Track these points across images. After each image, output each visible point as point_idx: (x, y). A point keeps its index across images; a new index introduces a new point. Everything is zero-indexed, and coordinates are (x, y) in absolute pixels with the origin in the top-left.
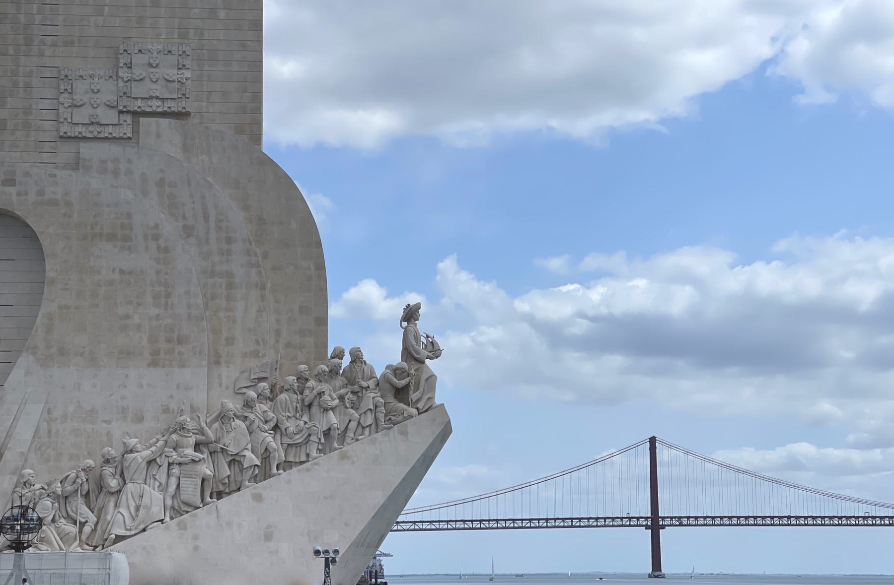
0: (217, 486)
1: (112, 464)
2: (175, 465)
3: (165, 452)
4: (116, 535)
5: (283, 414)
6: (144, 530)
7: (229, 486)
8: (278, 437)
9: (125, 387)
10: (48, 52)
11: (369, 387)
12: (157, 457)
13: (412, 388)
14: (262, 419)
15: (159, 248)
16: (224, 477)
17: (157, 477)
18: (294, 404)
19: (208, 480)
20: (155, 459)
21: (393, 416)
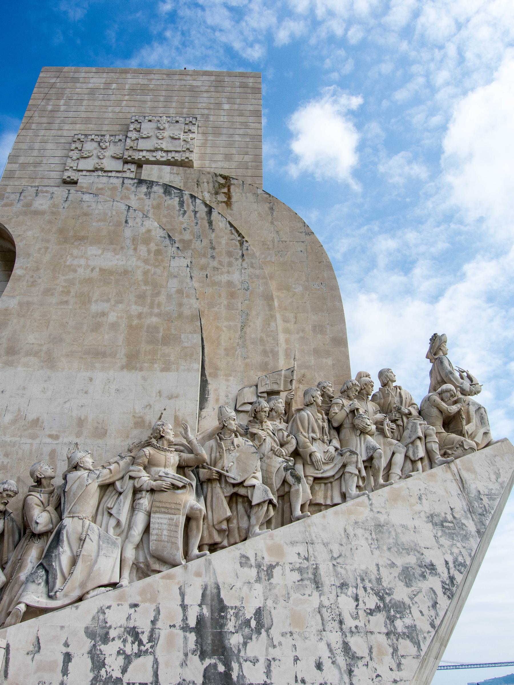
0: (210, 535)
1: (45, 488)
2: (144, 493)
3: (130, 471)
4: (27, 606)
5: (306, 434)
6: (80, 599)
7: (228, 536)
8: (299, 467)
9: (86, 392)
10: (67, 127)
11: (410, 414)
12: (118, 480)
13: (464, 417)
14: (276, 439)
15: (149, 252)
16: (221, 519)
17: (113, 512)
18: (320, 422)
19: (197, 519)
20: (112, 484)
21: (449, 449)
